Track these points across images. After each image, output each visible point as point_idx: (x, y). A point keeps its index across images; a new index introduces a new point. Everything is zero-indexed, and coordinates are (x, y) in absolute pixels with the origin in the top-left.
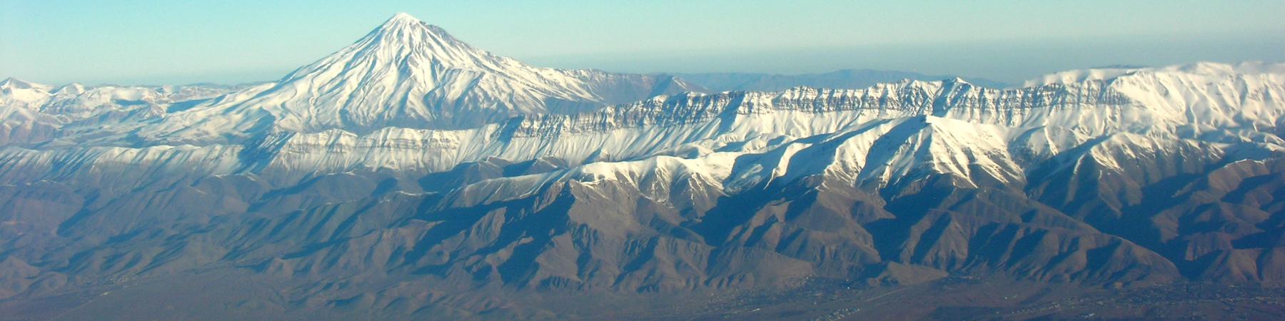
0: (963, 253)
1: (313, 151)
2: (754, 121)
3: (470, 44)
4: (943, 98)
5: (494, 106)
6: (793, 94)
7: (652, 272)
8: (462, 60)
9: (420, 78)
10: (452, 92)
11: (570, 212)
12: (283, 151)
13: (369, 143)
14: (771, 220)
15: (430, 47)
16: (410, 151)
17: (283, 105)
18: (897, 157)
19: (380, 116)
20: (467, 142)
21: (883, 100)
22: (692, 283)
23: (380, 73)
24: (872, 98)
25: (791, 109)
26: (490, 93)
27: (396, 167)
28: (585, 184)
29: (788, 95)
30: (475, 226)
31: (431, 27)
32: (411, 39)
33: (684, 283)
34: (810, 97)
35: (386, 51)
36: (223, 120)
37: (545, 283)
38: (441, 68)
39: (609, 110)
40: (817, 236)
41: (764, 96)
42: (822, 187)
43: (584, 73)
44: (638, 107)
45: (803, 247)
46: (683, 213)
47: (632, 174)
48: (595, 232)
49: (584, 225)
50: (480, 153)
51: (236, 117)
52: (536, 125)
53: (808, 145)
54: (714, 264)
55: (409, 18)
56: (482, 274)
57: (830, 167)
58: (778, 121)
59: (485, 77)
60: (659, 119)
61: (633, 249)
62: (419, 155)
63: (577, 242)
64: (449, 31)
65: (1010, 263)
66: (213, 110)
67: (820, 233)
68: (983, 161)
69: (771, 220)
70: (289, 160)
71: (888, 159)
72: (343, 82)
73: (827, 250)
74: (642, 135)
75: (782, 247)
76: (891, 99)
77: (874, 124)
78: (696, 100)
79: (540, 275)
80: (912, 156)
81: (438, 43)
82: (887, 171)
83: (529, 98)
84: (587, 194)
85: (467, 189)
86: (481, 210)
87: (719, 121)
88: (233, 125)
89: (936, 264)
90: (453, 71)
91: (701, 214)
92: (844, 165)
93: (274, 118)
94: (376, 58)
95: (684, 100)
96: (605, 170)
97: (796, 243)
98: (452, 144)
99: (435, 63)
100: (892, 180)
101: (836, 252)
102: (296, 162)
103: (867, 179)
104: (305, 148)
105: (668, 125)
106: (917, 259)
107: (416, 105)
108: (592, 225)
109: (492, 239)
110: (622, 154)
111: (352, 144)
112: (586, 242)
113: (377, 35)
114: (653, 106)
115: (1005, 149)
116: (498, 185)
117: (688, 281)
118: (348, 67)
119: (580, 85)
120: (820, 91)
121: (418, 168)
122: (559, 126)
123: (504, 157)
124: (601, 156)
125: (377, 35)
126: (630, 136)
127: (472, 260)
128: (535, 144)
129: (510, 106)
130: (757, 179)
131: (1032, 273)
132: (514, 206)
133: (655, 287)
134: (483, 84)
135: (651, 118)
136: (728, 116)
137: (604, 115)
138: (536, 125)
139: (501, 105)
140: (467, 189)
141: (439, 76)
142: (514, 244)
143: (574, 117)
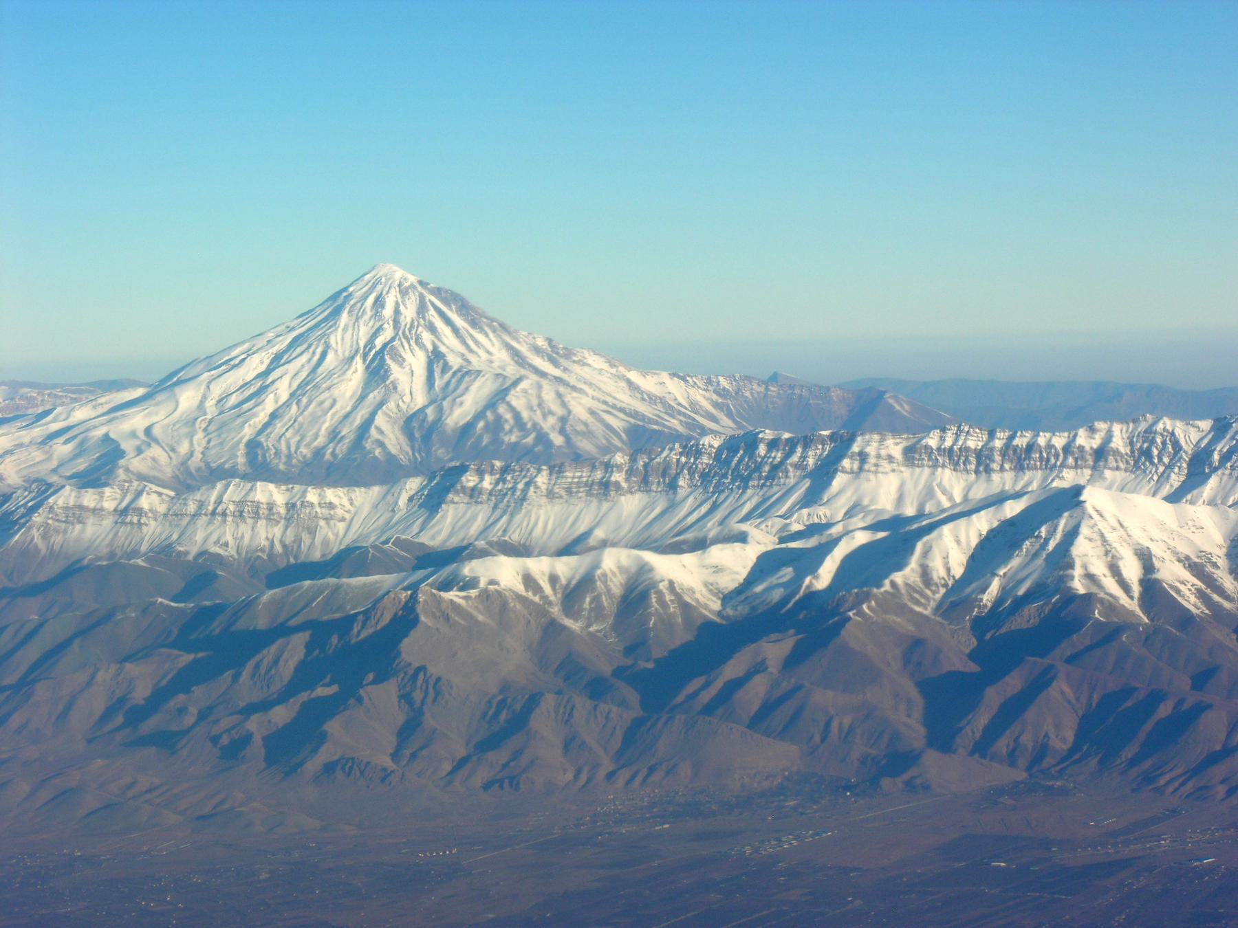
0: (1063, 737)
1: (91, 520)
2: (866, 486)
3: (509, 322)
4: (1208, 451)
5: (530, 439)
6: (942, 439)
7: (515, 756)
8: (490, 353)
9: (404, 386)
10: (457, 412)
11: (405, 644)
12: (37, 518)
13: (192, 507)
14: (758, 668)
15: (432, 328)
16: (262, 523)
17: (148, 431)
18: (1015, 562)
19: (319, 453)
20: (366, 510)
21: (1101, 454)
22: (584, 776)
23: (330, 374)
24: (1081, 448)
25: (935, 466)
26: (525, 415)
27: (232, 551)
28: (453, 595)
29: (932, 441)
30: (250, 665)
31: (437, 292)
32: (397, 312)
33: (570, 776)
34: (971, 444)
35: (347, 335)
36: (38, 455)
37: (329, 768)
38: (446, 367)
39: (619, 458)
40: (824, 698)
41: (890, 442)
42: (860, 613)
43: (724, 383)
44: (673, 454)
45: (795, 717)
46: (629, 650)
47: (553, 579)
48: (438, 680)
49: (422, 668)
50: (387, 526)
51: (62, 449)
52: (488, 482)
53: (881, 535)
54: (634, 740)
55: (399, 274)
56: (234, 750)
57: (898, 577)
58: (909, 485)
59: (523, 385)
60: (705, 476)
61: (496, 714)
62: (277, 531)
63: (406, 698)
64: (474, 300)
65: (1133, 762)
66: (26, 436)
67: (830, 694)
68: (1171, 573)
69: (758, 668)
70: (45, 537)
71: (998, 566)
72: (263, 389)
73: (835, 725)
74: (672, 507)
75: (758, 720)
76: (1116, 453)
77: (998, 500)
78: (773, 444)
79: (326, 754)
80: (1040, 561)
81: (448, 321)
82: (995, 586)
83: (597, 428)
84: (446, 613)
85: (265, 598)
86: (281, 631)
87: (807, 483)
88: (54, 464)
89: (1011, 759)
90: (466, 374)
91: (658, 653)
92: (925, 573)
93: (121, 454)
94: (327, 346)
95: (751, 443)
96: (505, 573)
97: (787, 709)
98: (339, 512)
99: (436, 358)
100: (998, 602)
101: (851, 729)
102: (57, 540)
103: (958, 598)
104: (77, 514)
105: (719, 489)
106: (982, 748)
107: (389, 436)
108: (434, 670)
109: (277, 686)
110: (557, 541)
111: (162, 509)
112: (421, 693)
113: (336, 304)
114: (698, 453)
115: (1221, 552)
116: (319, 591)
117: (578, 772)
118: (277, 361)
119: (716, 405)
120: (992, 435)
121: (272, 555)
122: (528, 485)
123: (424, 539)
124: (592, 541)
125: (336, 304)
126: (649, 507)
127: (226, 722)
128: (481, 514)
129: (558, 440)
130: (777, 595)
131: (1162, 781)
132: (319, 630)
133: (513, 781)
134: (517, 400)
135: (691, 474)
136: (823, 474)
137: (608, 467)
138: (488, 482)
139: (542, 438)
140: (265, 598)
141: (439, 383)
142: (304, 696)
143: (556, 470)
